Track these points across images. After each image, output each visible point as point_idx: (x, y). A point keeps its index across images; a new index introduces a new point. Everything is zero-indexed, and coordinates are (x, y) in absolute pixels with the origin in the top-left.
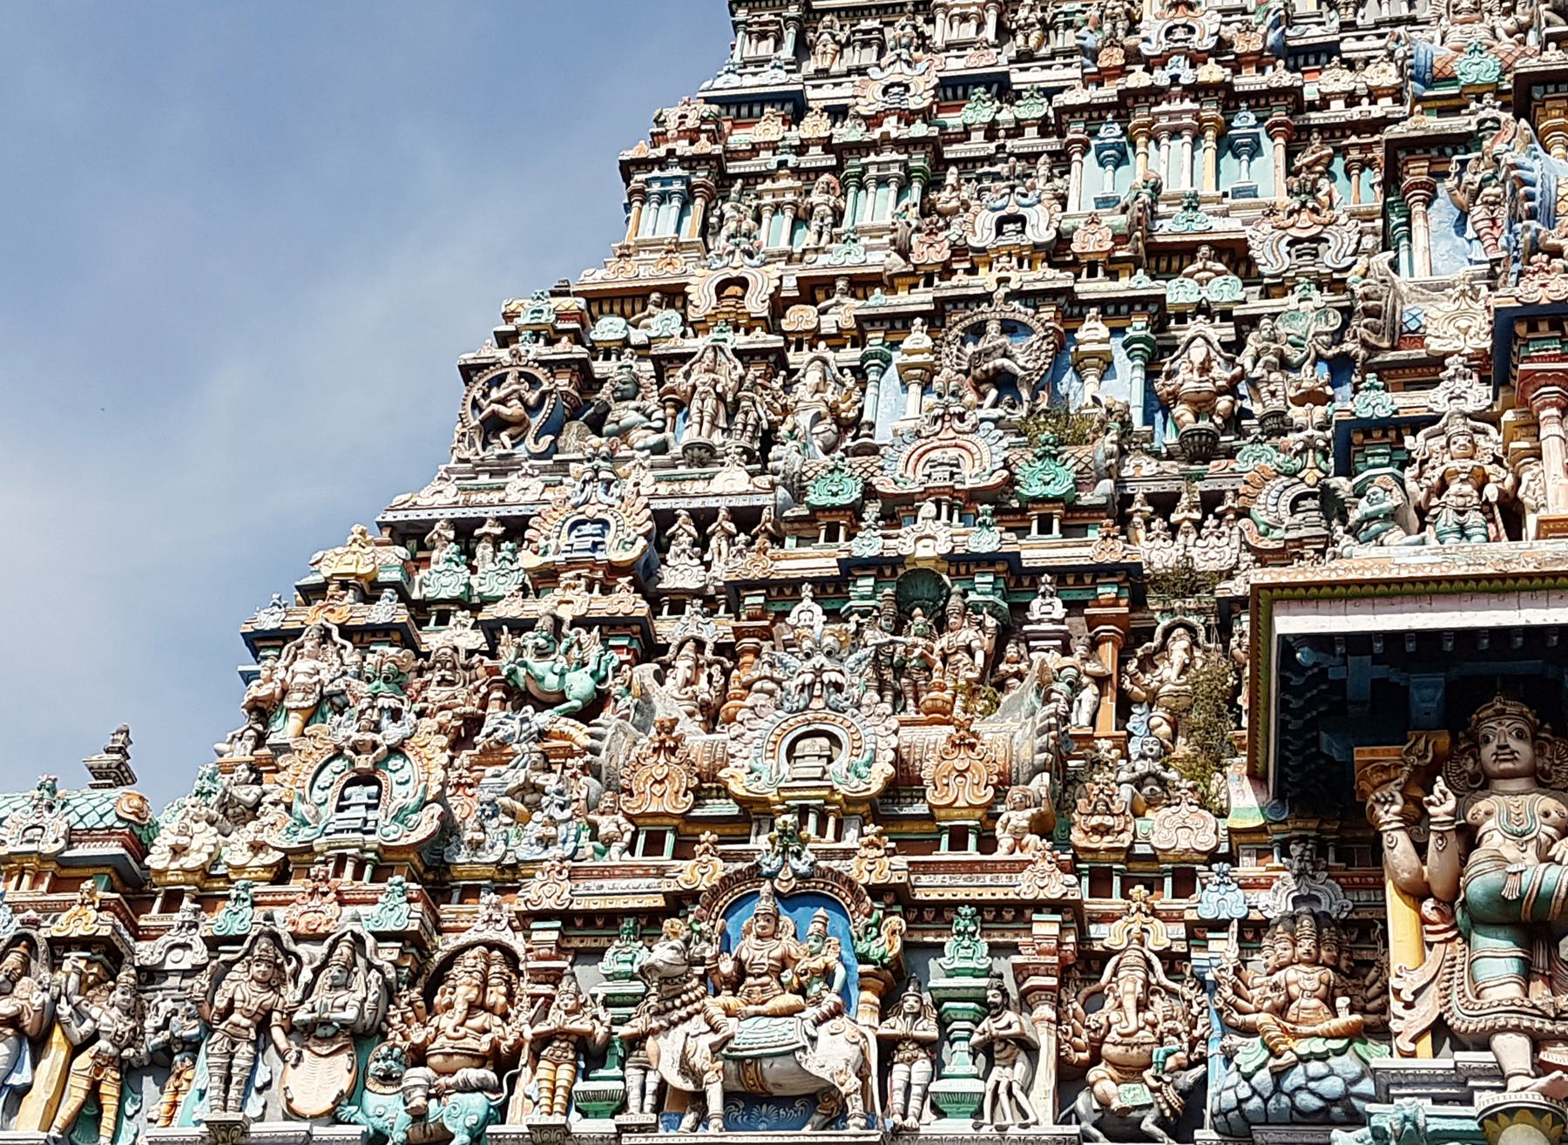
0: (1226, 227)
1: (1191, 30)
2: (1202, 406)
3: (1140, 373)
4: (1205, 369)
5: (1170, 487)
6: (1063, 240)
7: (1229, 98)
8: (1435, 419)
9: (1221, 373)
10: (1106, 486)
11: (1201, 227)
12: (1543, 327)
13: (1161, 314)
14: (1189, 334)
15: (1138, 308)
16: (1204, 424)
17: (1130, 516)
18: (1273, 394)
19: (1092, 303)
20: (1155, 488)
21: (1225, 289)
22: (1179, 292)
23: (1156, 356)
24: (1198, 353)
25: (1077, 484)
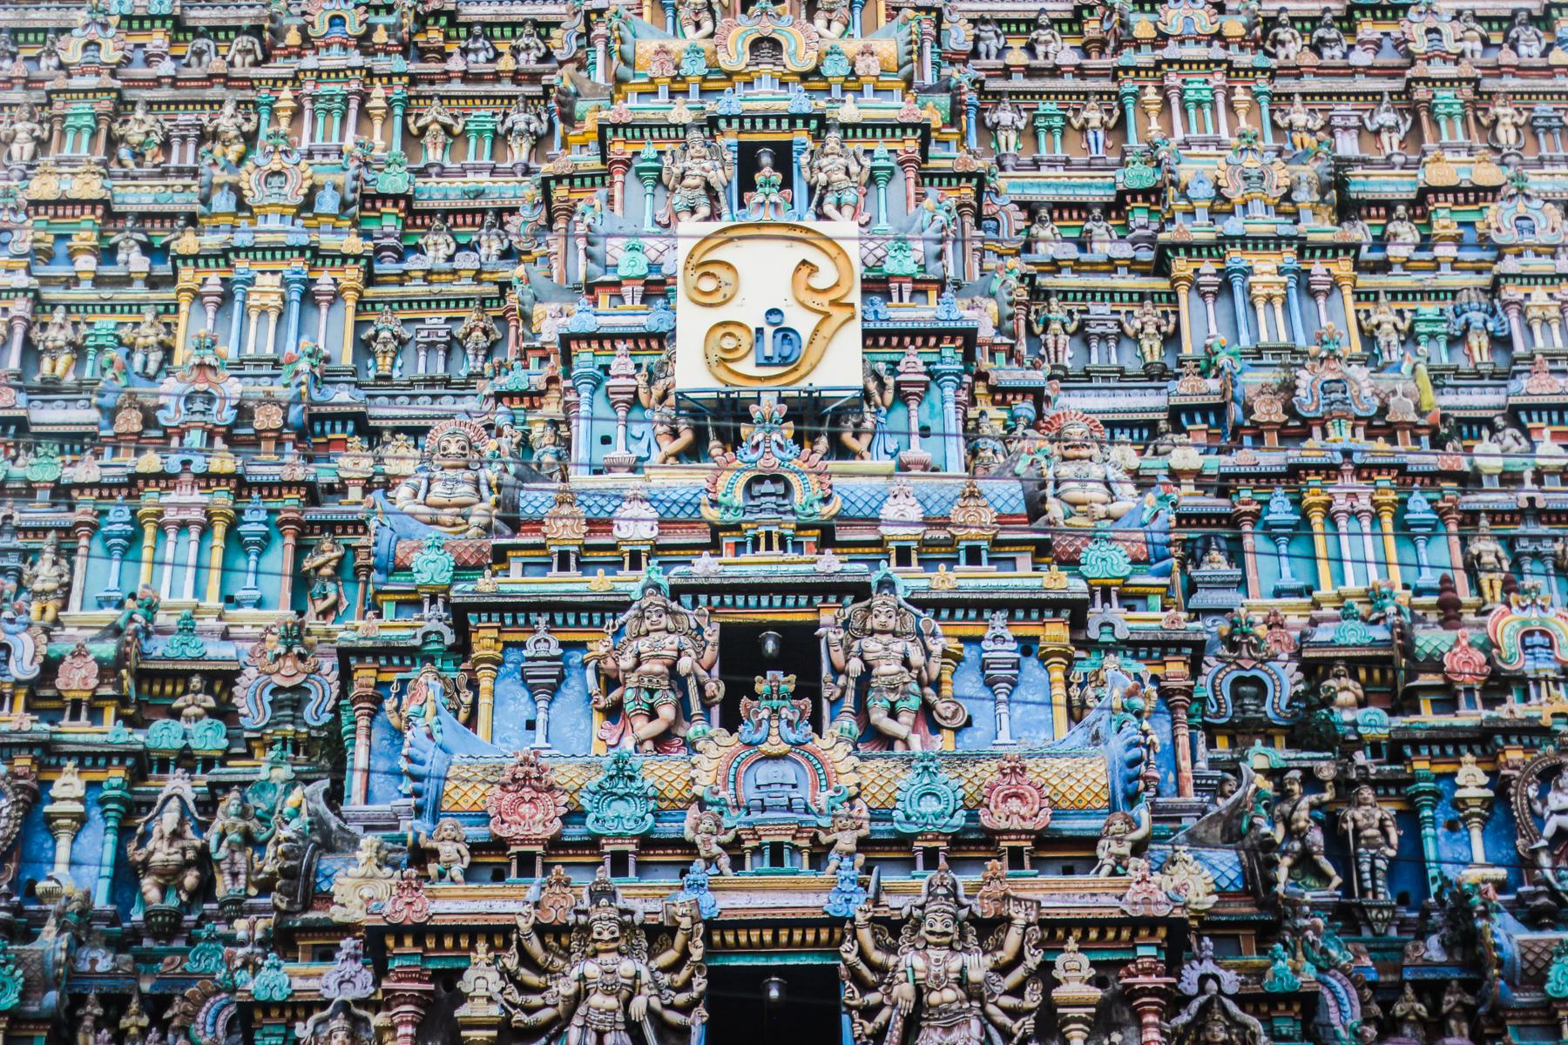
0: (219, 652)
1: (211, 399)
2: (170, 878)
3: (111, 838)
4: (177, 835)
5: (123, 985)
6: (50, 667)
7: (241, 485)
8: (324, 1005)
9: (193, 839)
10: (52, 997)
11: (195, 653)
12: (408, 942)
13: (143, 764)
14: (166, 792)
15: (115, 762)
16: (172, 902)
17: (81, 1019)
18: (235, 876)
19: (70, 755)
20: (107, 986)
21: (209, 738)
22: (163, 735)
23: (131, 816)
24: (170, 820)
25: (23, 996)
